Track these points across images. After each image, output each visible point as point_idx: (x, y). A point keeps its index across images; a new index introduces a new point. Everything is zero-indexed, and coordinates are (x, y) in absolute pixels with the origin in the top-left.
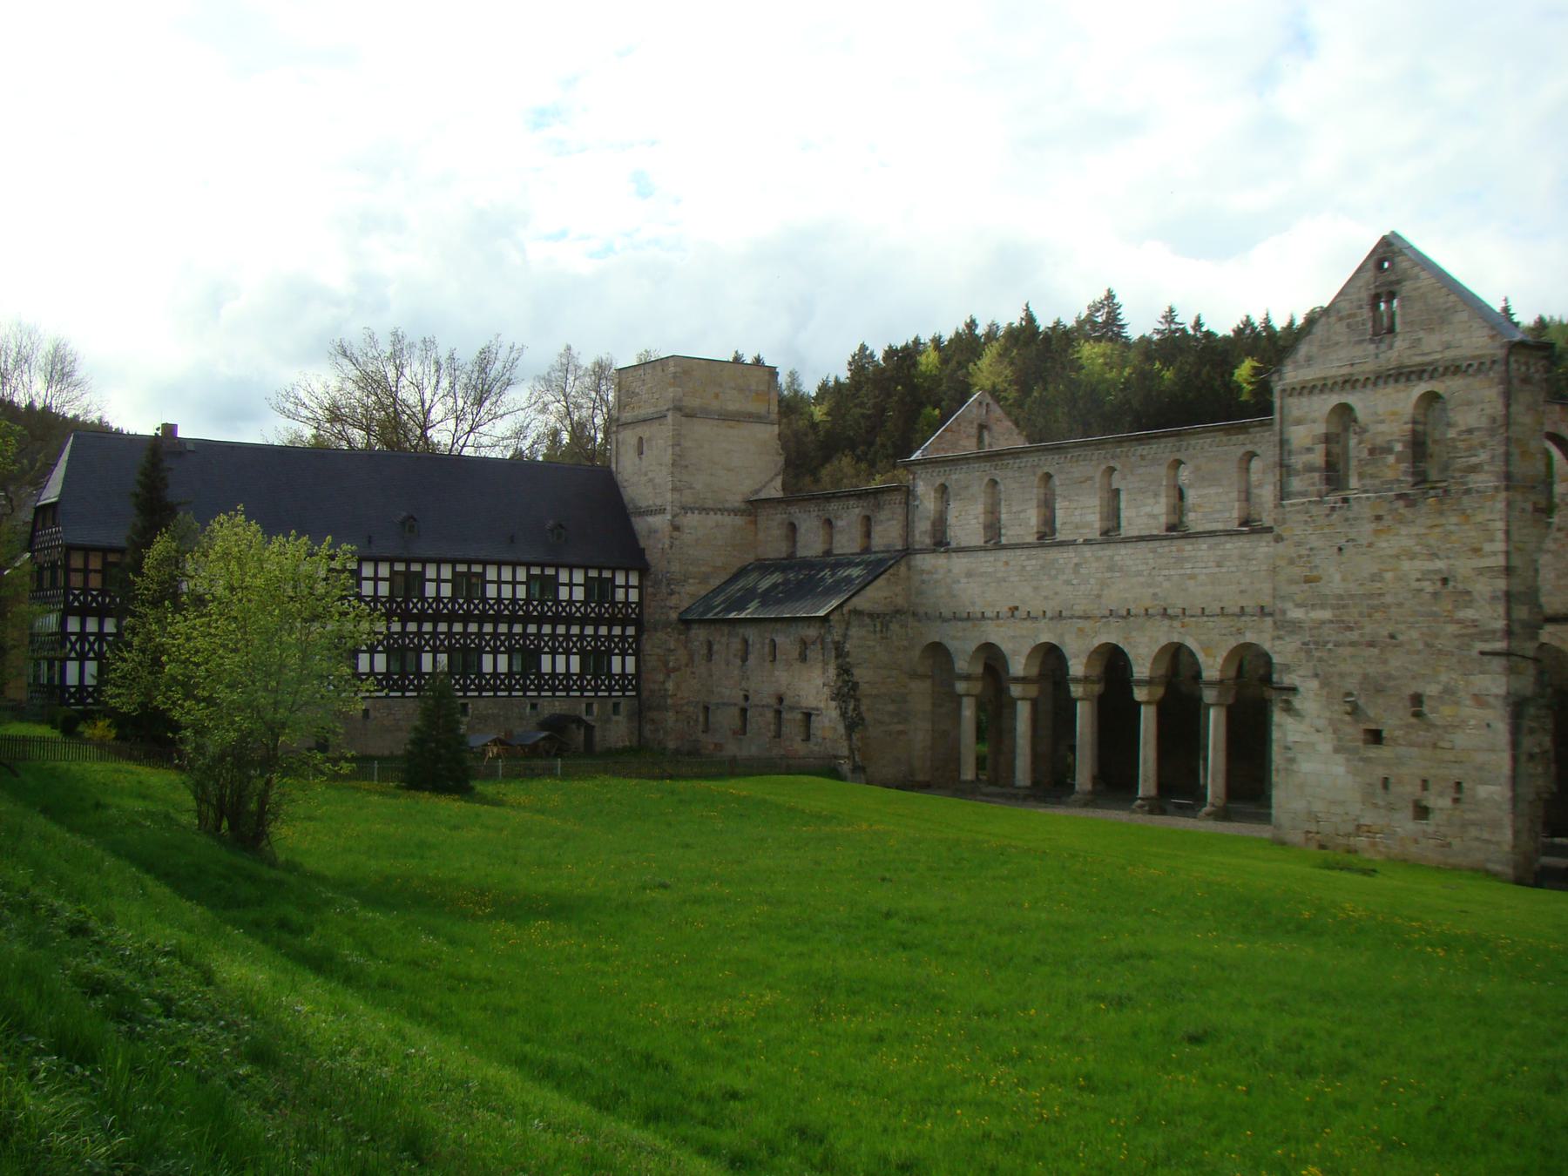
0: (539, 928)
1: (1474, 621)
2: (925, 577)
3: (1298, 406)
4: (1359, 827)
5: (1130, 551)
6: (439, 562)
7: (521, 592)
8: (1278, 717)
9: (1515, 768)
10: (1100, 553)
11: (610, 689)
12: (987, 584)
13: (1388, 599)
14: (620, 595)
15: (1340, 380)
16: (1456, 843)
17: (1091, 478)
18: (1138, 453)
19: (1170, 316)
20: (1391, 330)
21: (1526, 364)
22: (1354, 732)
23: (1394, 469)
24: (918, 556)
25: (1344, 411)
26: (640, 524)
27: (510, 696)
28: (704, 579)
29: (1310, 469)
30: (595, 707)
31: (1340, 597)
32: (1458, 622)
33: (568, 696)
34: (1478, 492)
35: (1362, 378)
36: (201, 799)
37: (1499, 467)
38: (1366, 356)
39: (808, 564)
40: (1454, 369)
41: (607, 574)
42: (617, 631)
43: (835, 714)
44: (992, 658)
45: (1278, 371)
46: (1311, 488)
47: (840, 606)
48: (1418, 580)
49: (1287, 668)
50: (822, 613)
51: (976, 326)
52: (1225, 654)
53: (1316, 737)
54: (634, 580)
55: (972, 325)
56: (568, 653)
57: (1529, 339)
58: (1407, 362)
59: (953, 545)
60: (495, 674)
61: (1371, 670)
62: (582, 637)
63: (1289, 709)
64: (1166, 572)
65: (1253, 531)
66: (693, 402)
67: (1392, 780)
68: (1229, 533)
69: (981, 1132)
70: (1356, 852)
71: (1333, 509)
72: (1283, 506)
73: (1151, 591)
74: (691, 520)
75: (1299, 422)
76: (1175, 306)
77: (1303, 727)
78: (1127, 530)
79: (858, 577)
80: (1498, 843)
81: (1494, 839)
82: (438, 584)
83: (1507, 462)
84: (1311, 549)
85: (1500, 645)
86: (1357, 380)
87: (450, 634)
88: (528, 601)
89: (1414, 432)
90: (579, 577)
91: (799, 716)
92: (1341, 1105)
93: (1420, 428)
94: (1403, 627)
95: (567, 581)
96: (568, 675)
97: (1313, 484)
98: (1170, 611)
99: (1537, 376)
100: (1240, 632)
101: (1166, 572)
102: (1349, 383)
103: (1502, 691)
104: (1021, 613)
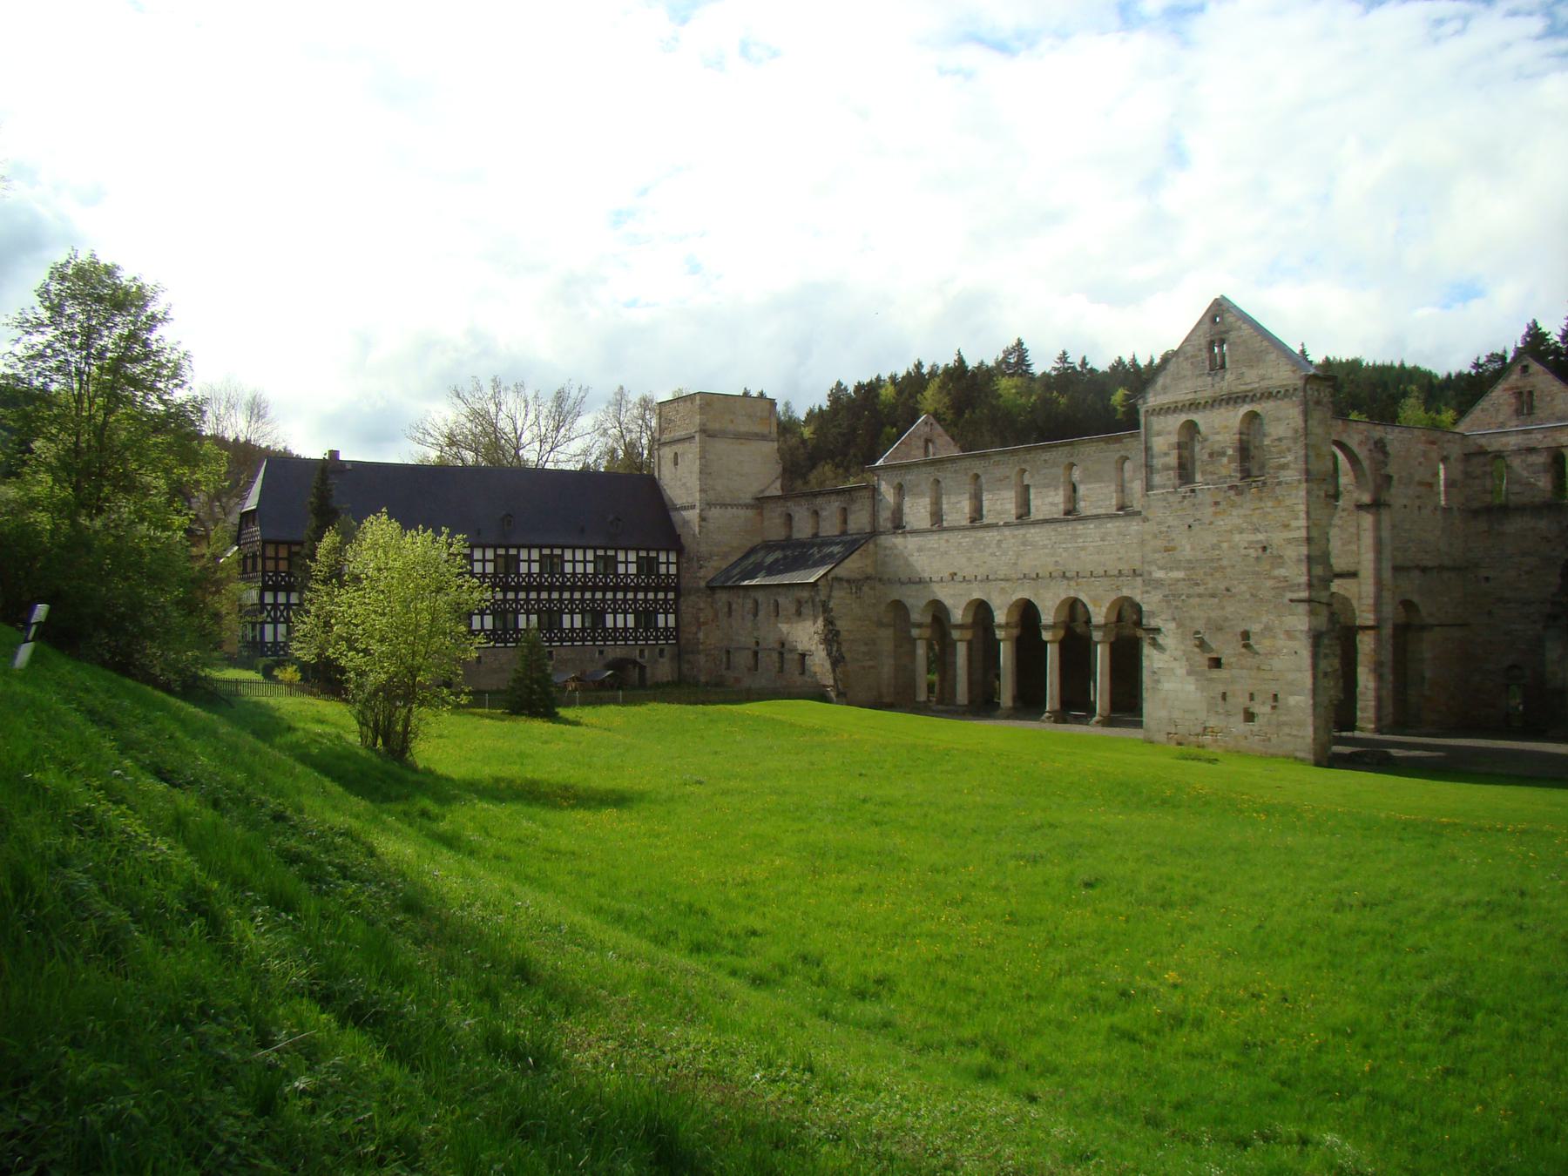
0: (609, 814)
1: (1285, 577)
2: (888, 552)
3: (1158, 423)
4: (1205, 728)
5: (1038, 530)
6: (529, 547)
7: (590, 568)
8: (1147, 650)
9: (1314, 684)
10: (1016, 532)
11: (657, 639)
12: (934, 556)
13: (1225, 563)
14: (663, 569)
15: (1187, 403)
16: (1274, 739)
17: (1008, 477)
18: (1043, 458)
19: (1063, 357)
20: (1223, 367)
21: (1317, 390)
22: (1202, 660)
23: (1228, 467)
24: (883, 537)
25: (1191, 428)
26: (675, 516)
27: (583, 645)
28: (725, 556)
29: (1167, 468)
30: (646, 653)
31: (1189, 561)
32: (1275, 578)
33: (626, 644)
34: (1286, 483)
35: (1203, 402)
36: (362, 724)
37: (1301, 465)
38: (1204, 386)
39: (802, 544)
40: (1268, 395)
41: (653, 554)
42: (661, 595)
43: (823, 654)
44: (939, 612)
45: (1143, 397)
46: (1168, 483)
47: (826, 574)
48: (1245, 548)
49: (1152, 614)
50: (812, 580)
51: (922, 366)
52: (1108, 605)
53: (1175, 665)
54: (673, 558)
55: (919, 366)
56: (625, 612)
57: (1320, 374)
58: (1234, 390)
59: (908, 528)
60: (572, 629)
61: (1213, 615)
62: (635, 600)
63: (1155, 644)
64: (1064, 546)
65: (1127, 515)
66: (714, 426)
67: (1228, 694)
68: (1110, 517)
69: (934, 956)
70: (1203, 747)
71: (1184, 497)
72: (1148, 496)
73: (1054, 559)
74: (715, 513)
75: (1159, 434)
76: (1067, 350)
77: (1165, 657)
78: (1036, 514)
79: (838, 553)
80: (1303, 737)
81: (1300, 734)
82: (530, 563)
83: (1306, 462)
84: (1169, 527)
85: (1304, 594)
86: (1199, 403)
87: (538, 600)
88: (595, 575)
89: (1241, 441)
90: (632, 556)
91: (796, 657)
92: (1193, 927)
93: (1244, 437)
94: (1236, 582)
95: (481, 558)
96: (626, 629)
97: (1169, 479)
98: (1067, 574)
99: (1325, 400)
100: (1118, 588)
101: (1064, 546)
102: (1194, 406)
103: (1305, 627)
104: (959, 578)
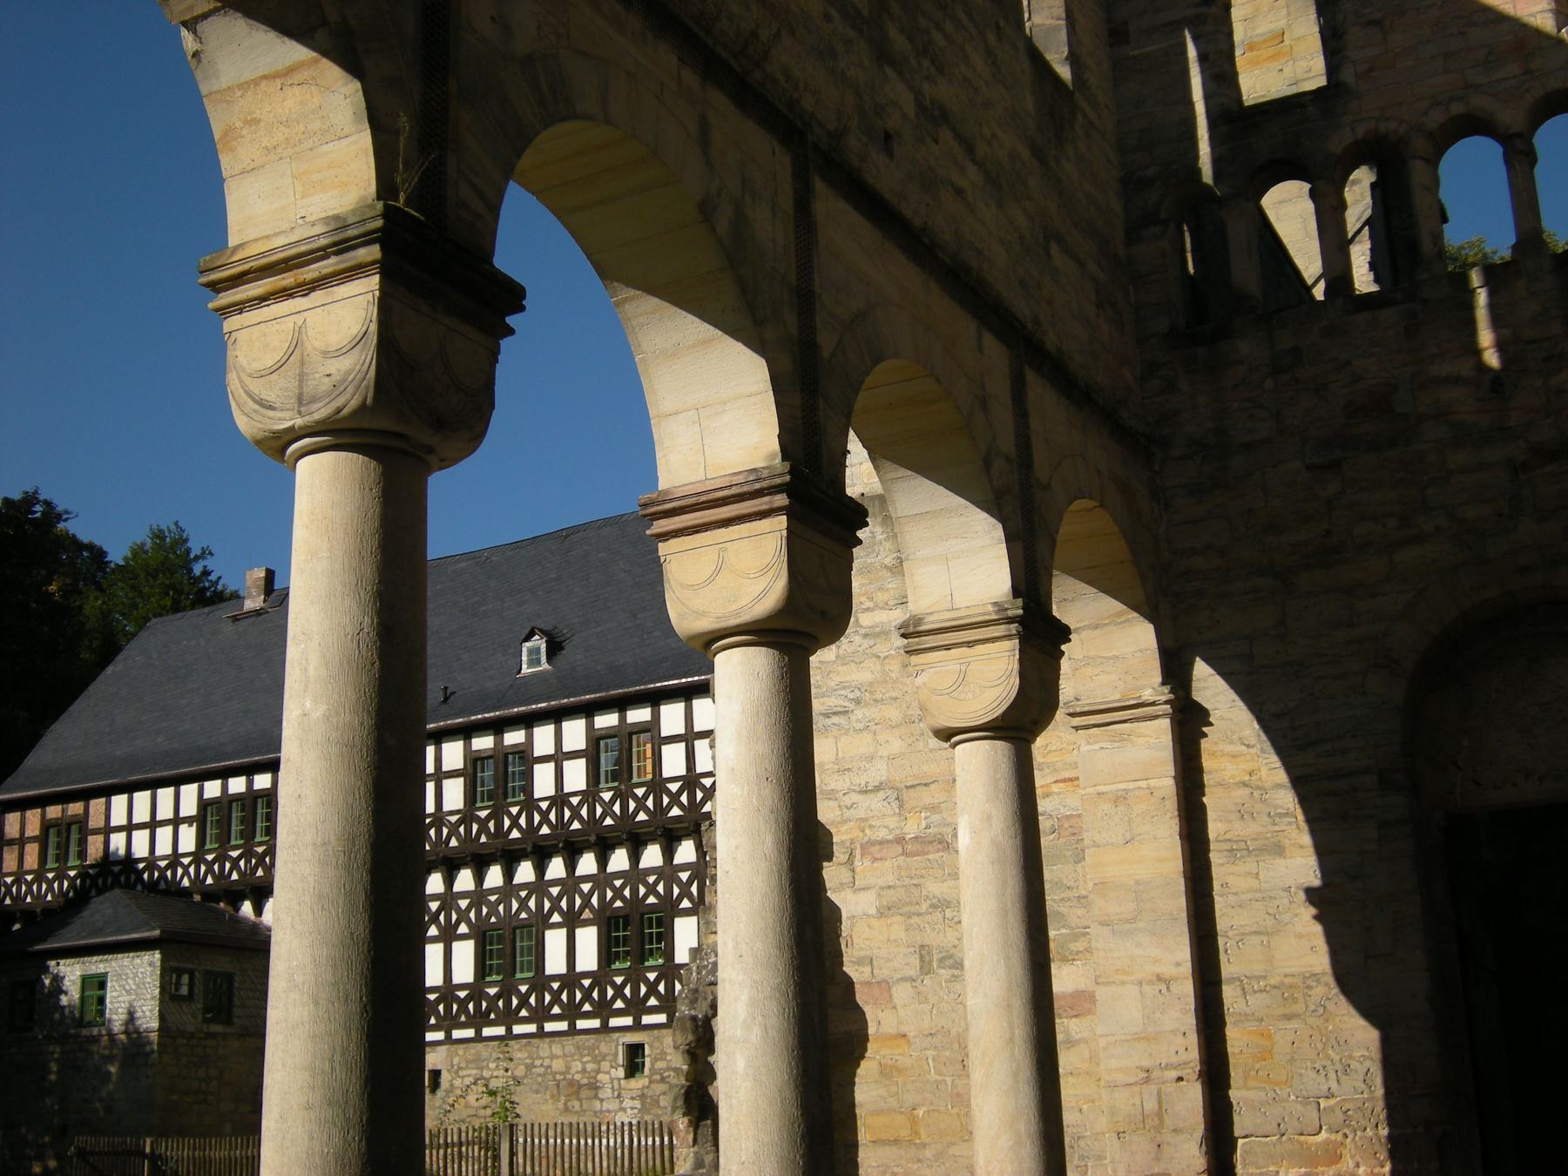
6: (556, 716)
